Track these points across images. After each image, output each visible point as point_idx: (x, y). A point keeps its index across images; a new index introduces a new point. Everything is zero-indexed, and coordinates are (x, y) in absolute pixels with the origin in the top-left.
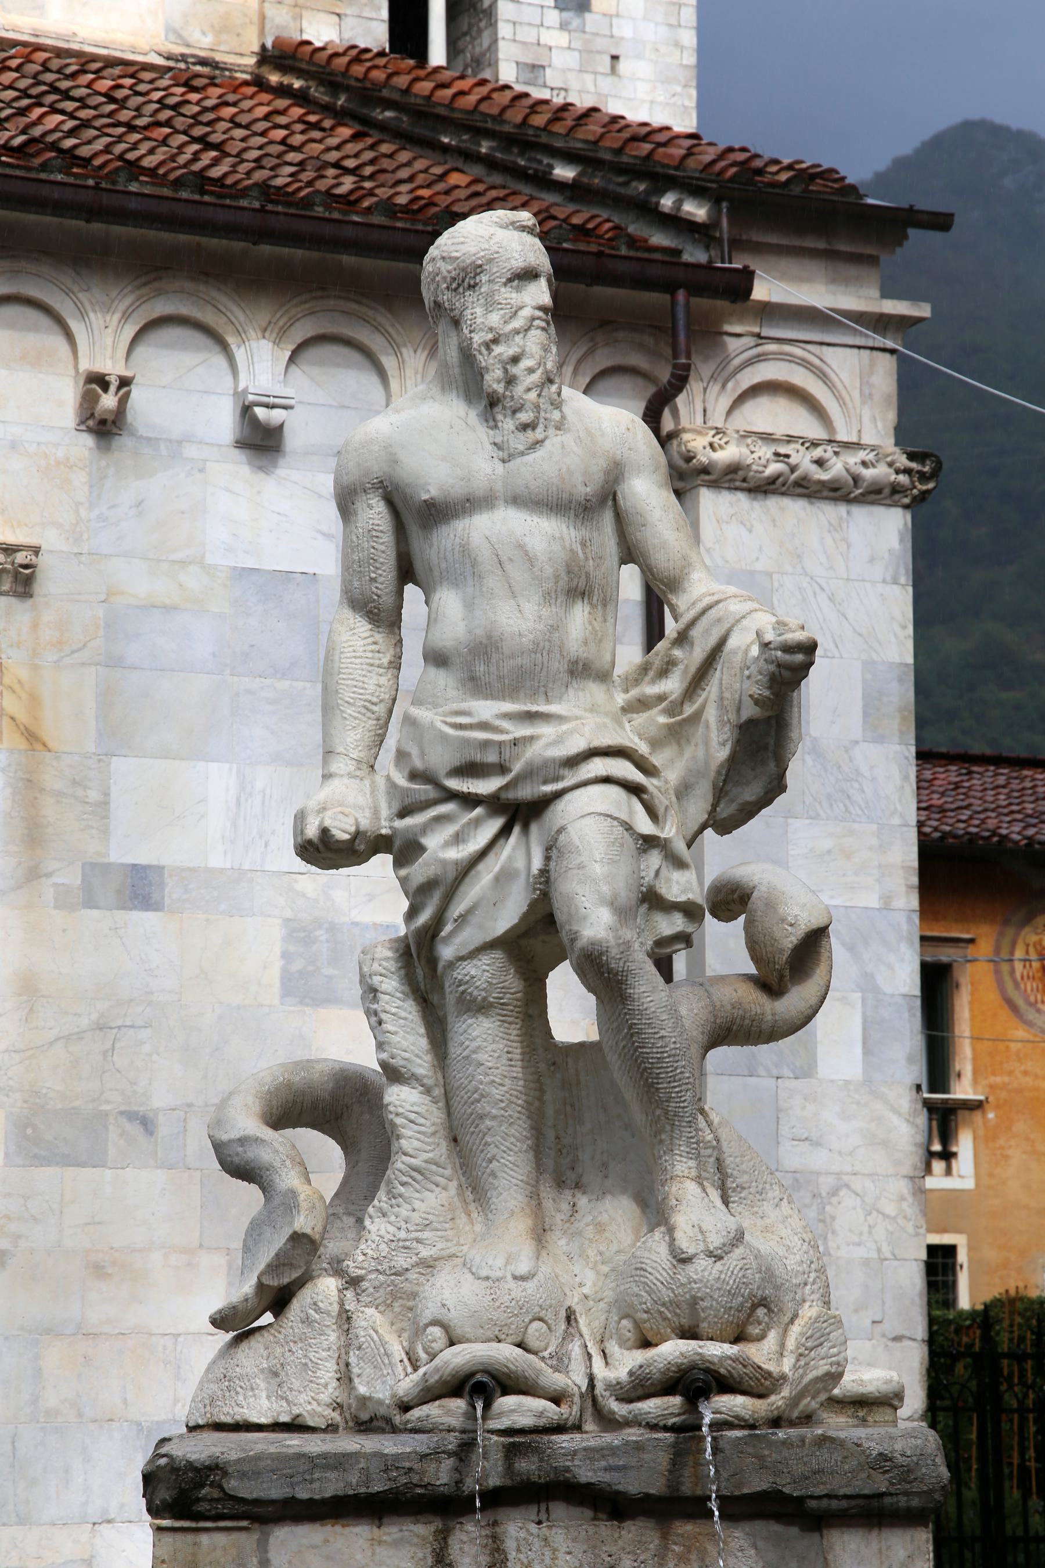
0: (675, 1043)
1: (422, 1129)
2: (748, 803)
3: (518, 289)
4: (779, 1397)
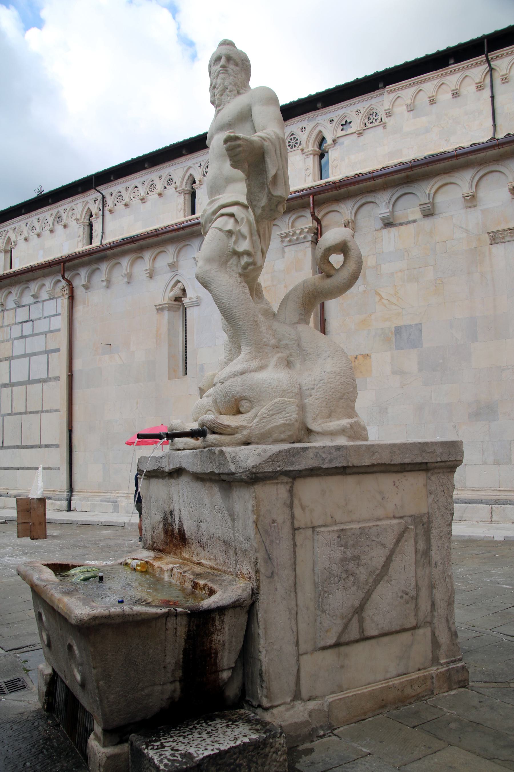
0: (229, 304)
1: (227, 349)
2: (263, 207)
3: (217, 65)
4: (239, 435)
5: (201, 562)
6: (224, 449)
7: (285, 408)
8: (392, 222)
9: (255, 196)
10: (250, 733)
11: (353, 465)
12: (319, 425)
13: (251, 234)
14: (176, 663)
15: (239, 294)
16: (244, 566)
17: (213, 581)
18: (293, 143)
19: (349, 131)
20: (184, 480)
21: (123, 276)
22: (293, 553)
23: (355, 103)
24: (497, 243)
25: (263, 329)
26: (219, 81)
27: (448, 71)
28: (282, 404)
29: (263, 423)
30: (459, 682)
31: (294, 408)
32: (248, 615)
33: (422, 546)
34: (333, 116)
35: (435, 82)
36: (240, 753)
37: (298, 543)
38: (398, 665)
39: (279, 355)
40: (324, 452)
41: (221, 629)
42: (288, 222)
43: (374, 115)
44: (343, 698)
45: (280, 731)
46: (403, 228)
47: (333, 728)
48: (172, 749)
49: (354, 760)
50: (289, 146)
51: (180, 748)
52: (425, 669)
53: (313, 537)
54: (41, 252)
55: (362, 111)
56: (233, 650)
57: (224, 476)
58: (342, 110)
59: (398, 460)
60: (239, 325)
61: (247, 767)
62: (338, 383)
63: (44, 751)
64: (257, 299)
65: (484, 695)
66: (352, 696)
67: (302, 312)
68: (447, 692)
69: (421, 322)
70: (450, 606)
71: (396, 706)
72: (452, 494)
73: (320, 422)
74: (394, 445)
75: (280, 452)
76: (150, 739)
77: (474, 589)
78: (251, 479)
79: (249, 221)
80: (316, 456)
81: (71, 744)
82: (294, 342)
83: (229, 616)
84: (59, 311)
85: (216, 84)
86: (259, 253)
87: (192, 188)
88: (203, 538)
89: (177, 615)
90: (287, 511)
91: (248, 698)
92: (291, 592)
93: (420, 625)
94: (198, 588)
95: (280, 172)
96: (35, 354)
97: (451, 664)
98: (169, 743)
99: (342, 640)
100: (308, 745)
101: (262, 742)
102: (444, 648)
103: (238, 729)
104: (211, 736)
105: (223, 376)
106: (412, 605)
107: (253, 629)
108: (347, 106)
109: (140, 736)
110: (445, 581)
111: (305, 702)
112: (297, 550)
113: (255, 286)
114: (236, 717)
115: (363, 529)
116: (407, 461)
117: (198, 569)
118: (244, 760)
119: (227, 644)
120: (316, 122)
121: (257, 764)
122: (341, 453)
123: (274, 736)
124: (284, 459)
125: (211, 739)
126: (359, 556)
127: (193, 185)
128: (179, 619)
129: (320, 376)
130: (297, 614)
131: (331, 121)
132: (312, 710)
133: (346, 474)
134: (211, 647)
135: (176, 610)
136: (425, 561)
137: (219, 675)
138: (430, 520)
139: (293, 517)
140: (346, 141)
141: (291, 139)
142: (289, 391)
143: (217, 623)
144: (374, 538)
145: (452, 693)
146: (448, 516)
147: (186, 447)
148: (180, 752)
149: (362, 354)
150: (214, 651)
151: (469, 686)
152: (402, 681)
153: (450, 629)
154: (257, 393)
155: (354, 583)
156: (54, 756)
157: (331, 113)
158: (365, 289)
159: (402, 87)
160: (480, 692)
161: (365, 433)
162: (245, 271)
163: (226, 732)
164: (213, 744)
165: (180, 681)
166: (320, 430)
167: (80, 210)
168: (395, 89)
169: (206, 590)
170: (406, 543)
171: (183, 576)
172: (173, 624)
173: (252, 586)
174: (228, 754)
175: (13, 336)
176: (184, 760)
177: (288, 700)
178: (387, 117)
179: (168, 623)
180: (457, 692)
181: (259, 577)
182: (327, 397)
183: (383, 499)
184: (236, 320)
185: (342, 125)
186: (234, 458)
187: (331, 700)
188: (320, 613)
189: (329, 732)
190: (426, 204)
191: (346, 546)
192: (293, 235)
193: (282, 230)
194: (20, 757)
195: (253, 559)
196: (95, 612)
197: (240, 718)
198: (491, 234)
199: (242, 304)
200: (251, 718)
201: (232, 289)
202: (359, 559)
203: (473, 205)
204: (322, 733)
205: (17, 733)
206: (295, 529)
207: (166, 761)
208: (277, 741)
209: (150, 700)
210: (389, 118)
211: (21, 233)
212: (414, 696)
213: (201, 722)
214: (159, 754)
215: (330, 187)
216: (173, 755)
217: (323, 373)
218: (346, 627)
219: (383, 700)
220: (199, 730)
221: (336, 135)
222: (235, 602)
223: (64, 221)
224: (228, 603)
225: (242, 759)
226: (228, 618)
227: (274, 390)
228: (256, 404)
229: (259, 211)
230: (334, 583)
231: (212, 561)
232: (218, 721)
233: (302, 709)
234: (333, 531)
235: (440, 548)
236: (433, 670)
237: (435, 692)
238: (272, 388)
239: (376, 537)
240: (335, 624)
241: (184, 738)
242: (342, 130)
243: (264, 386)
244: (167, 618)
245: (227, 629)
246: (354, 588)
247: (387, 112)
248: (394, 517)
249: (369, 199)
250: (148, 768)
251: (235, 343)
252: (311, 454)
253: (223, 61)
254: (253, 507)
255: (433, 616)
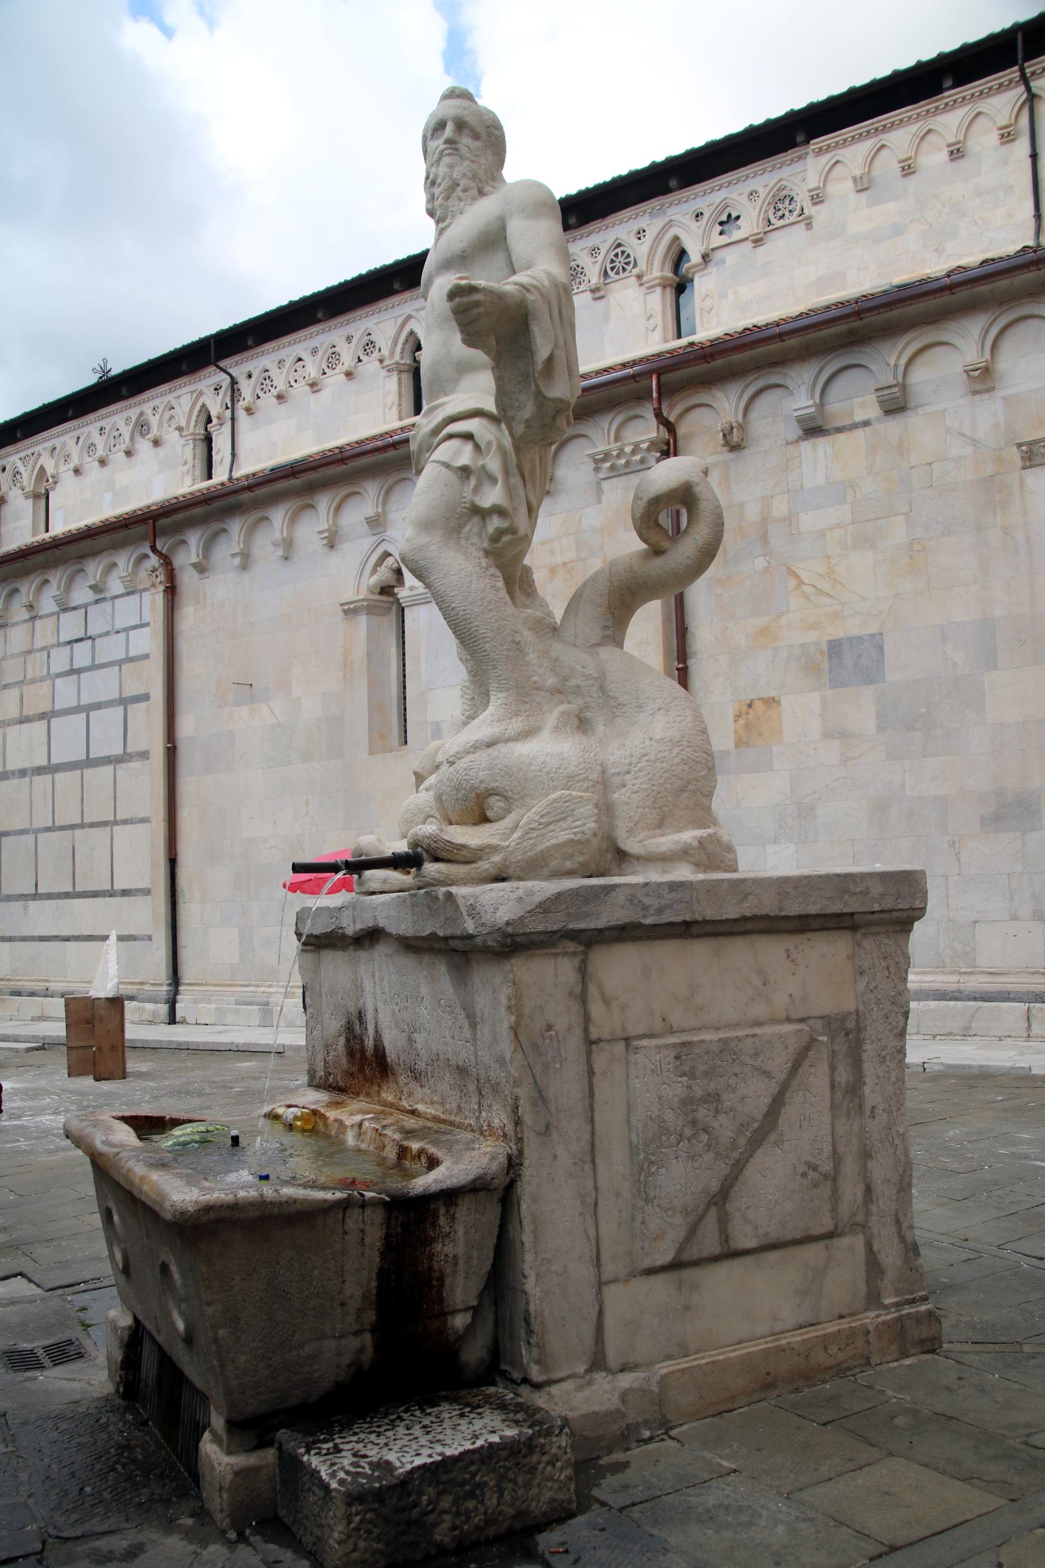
0: (464, 610)
2: (527, 421)
3: (438, 138)
5: (416, 1109)
6: (454, 890)
7: (573, 810)
8: (821, 427)
9: (511, 399)
10: (503, 1427)
11: (704, 918)
12: (641, 842)
13: (507, 473)
14: (364, 1296)
15: (483, 591)
16: (494, 1113)
17: (436, 1143)
18: (620, 262)
19: (736, 235)
20: (381, 951)
21: (275, 544)
22: (587, 1087)
23: (747, 177)
24: (1037, 466)
25: (532, 657)
26: (442, 170)
27: (941, 104)
28: (566, 802)
29: (530, 838)
30: (922, 1342)
31: (588, 810)
32: (502, 1206)
33: (844, 1075)
34: (702, 206)
35: (914, 128)
36: (482, 1462)
37: (597, 1070)
38: (799, 1306)
39: (564, 707)
40: (647, 895)
41: (449, 1233)
42: (609, 430)
43: (787, 202)
44: (689, 1367)
45: (559, 1423)
46: (842, 437)
47: (670, 1425)
48: (355, 1455)
49: (705, 1482)
50: (612, 269)
51: (369, 1453)
52: (852, 1315)
53: (626, 1058)
54: (108, 497)
55: (762, 193)
56: (474, 1273)
57: (455, 941)
58: (720, 192)
59: (794, 908)
60: (485, 651)
61: (495, 1489)
62: (676, 761)
63: (119, 1467)
64: (523, 598)
65: (969, 1366)
66: (707, 1363)
67: (609, 624)
68: (896, 1360)
69: (880, 631)
70: (902, 1194)
71: (795, 1386)
72: (904, 975)
73: (641, 836)
74: (786, 880)
75: (559, 895)
76: (315, 1438)
77: (974, 1168)
78: (504, 946)
79: (501, 448)
80: (631, 902)
81: (170, 1457)
82: (592, 682)
83: (465, 1208)
84: (146, 619)
85: (436, 176)
86: (523, 510)
87: (415, 360)
88: (420, 1063)
89: (364, 1204)
90: (576, 1007)
91: (503, 1367)
92: (584, 1162)
93: (842, 1230)
94: (409, 1156)
95: (560, 353)
96: (98, 706)
97: (906, 1307)
98: (349, 1444)
99: (686, 1256)
100: (618, 1456)
101: (524, 1443)
102: (890, 1275)
103: (481, 1421)
104: (428, 1433)
105: (453, 751)
106: (825, 1190)
107: (511, 1234)
108: (730, 183)
109: (295, 1433)
110: (892, 1144)
111: (613, 1374)
112: (596, 1081)
113: (519, 573)
114: (480, 1400)
115: (725, 1042)
116: (813, 910)
117: (410, 1123)
118: (491, 1475)
119: (461, 1262)
120: (669, 218)
121: (516, 1483)
122: (680, 896)
123: (549, 1433)
124: (567, 908)
125: (429, 1437)
126: (717, 1094)
127: (417, 354)
128: (369, 1212)
129: (642, 748)
130: (596, 1204)
131: (698, 216)
132: (627, 1389)
133: (693, 936)
134: (431, 1268)
135: (362, 1195)
136: (851, 1105)
137: (447, 1321)
138: (861, 1025)
139: (587, 1018)
140: (730, 256)
141: (616, 255)
142: (581, 777)
143: (442, 1221)
144: (748, 1060)
145: (907, 1362)
146: (897, 1017)
147: (386, 888)
148: (368, 1460)
149: (762, 696)
150: (437, 1274)
151: (943, 1349)
152: (805, 1337)
153: (902, 1238)
154: (519, 782)
155: (709, 1146)
156: (137, 1476)
157: (698, 200)
158: (766, 564)
159: (845, 140)
160: (961, 1360)
161: (731, 856)
162: (495, 546)
163: (459, 1425)
164: (431, 1445)
165: (372, 1331)
166: (642, 852)
167: (187, 408)
168: (829, 146)
169: (424, 1160)
170: (813, 1070)
171: (380, 1135)
172: (357, 1221)
173: (509, 1151)
174: (460, 1464)
175: (54, 670)
176: (376, 1474)
177: (581, 1369)
178: (814, 204)
179: (347, 1221)
180: (916, 1362)
181: (522, 1133)
182: (654, 788)
183: (765, 984)
184: (478, 640)
185: (721, 224)
186: (472, 907)
187: (664, 1371)
188: (642, 1203)
189: (660, 1432)
190: (890, 387)
191: (692, 1075)
192: (618, 456)
193: (596, 447)
194: (73, 1477)
195: (509, 1100)
196: (208, 1196)
197: (487, 1401)
198: (1023, 448)
199: (490, 610)
200: (508, 1402)
201: (471, 581)
202: (719, 1100)
203: (985, 387)
204: (647, 1434)
205: (66, 1437)
206: (592, 1043)
207: (342, 1475)
208: (555, 1442)
209: (316, 1367)
210: (818, 207)
211: (67, 457)
212: (830, 1368)
213: (412, 1409)
214: (329, 1462)
215: (692, 357)
216: (356, 1465)
217: (648, 742)
218: (692, 1232)
219: (768, 1374)
220: (408, 1422)
221: (708, 245)
222: (475, 1180)
223: (154, 432)
224: (462, 1183)
225: (487, 1475)
226: (463, 1211)
227: (551, 775)
228: (516, 803)
229: (520, 429)
230: (669, 1147)
231: (436, 1106)
232: (445, 1407)
233: (607, 1386)
234: (666, 1046)
235: (882, 1079)
236: (870, 1318)
237: (874, 1361)
238: (548, 773)
239: (751, 1057)
240: (672, 1224)
241: (378, 1436)
242: (721, 233)
243: (533, 768)
244: (345, 1210)
245: (461, 1232)
246: (709, 1157)
247: (812, 194)
248: (788, 1020)
249: (774, 380)
250: (310, 1489)
251: (481, 686)
252: (620, 897)
253: (449, 131)
254: (510, 999)
255: (868, 1213)
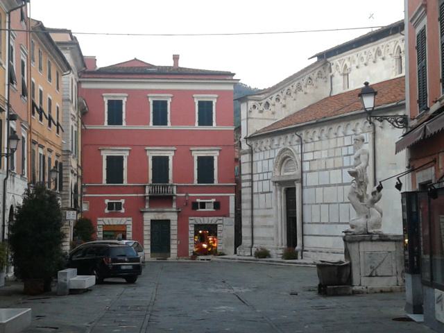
167: (393, 46)
175: (343, 154)
211: (354, 61)
223: (383, 55)
